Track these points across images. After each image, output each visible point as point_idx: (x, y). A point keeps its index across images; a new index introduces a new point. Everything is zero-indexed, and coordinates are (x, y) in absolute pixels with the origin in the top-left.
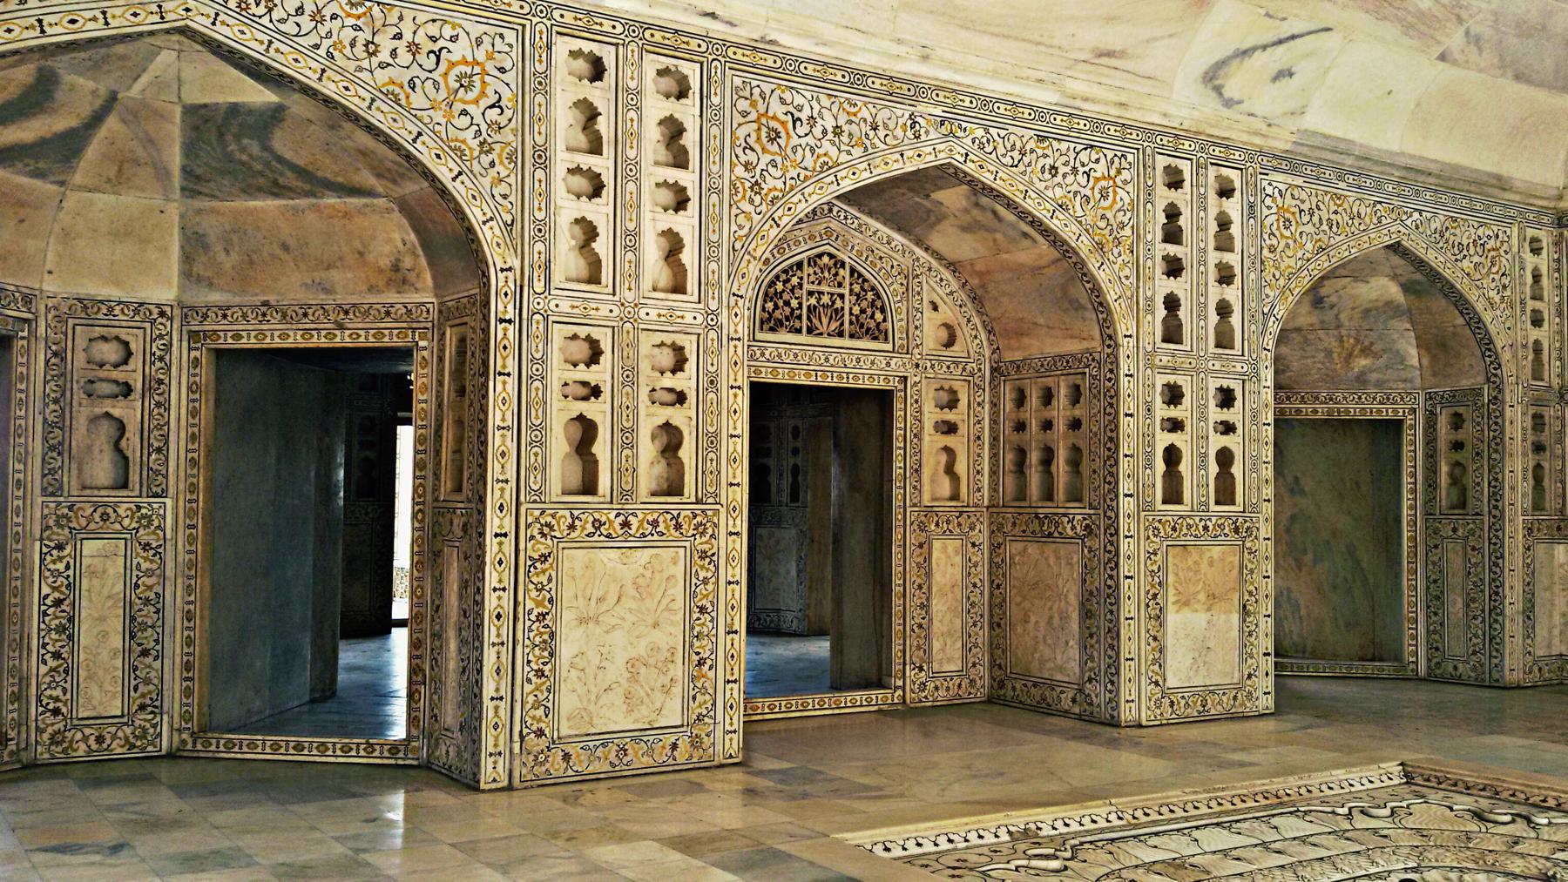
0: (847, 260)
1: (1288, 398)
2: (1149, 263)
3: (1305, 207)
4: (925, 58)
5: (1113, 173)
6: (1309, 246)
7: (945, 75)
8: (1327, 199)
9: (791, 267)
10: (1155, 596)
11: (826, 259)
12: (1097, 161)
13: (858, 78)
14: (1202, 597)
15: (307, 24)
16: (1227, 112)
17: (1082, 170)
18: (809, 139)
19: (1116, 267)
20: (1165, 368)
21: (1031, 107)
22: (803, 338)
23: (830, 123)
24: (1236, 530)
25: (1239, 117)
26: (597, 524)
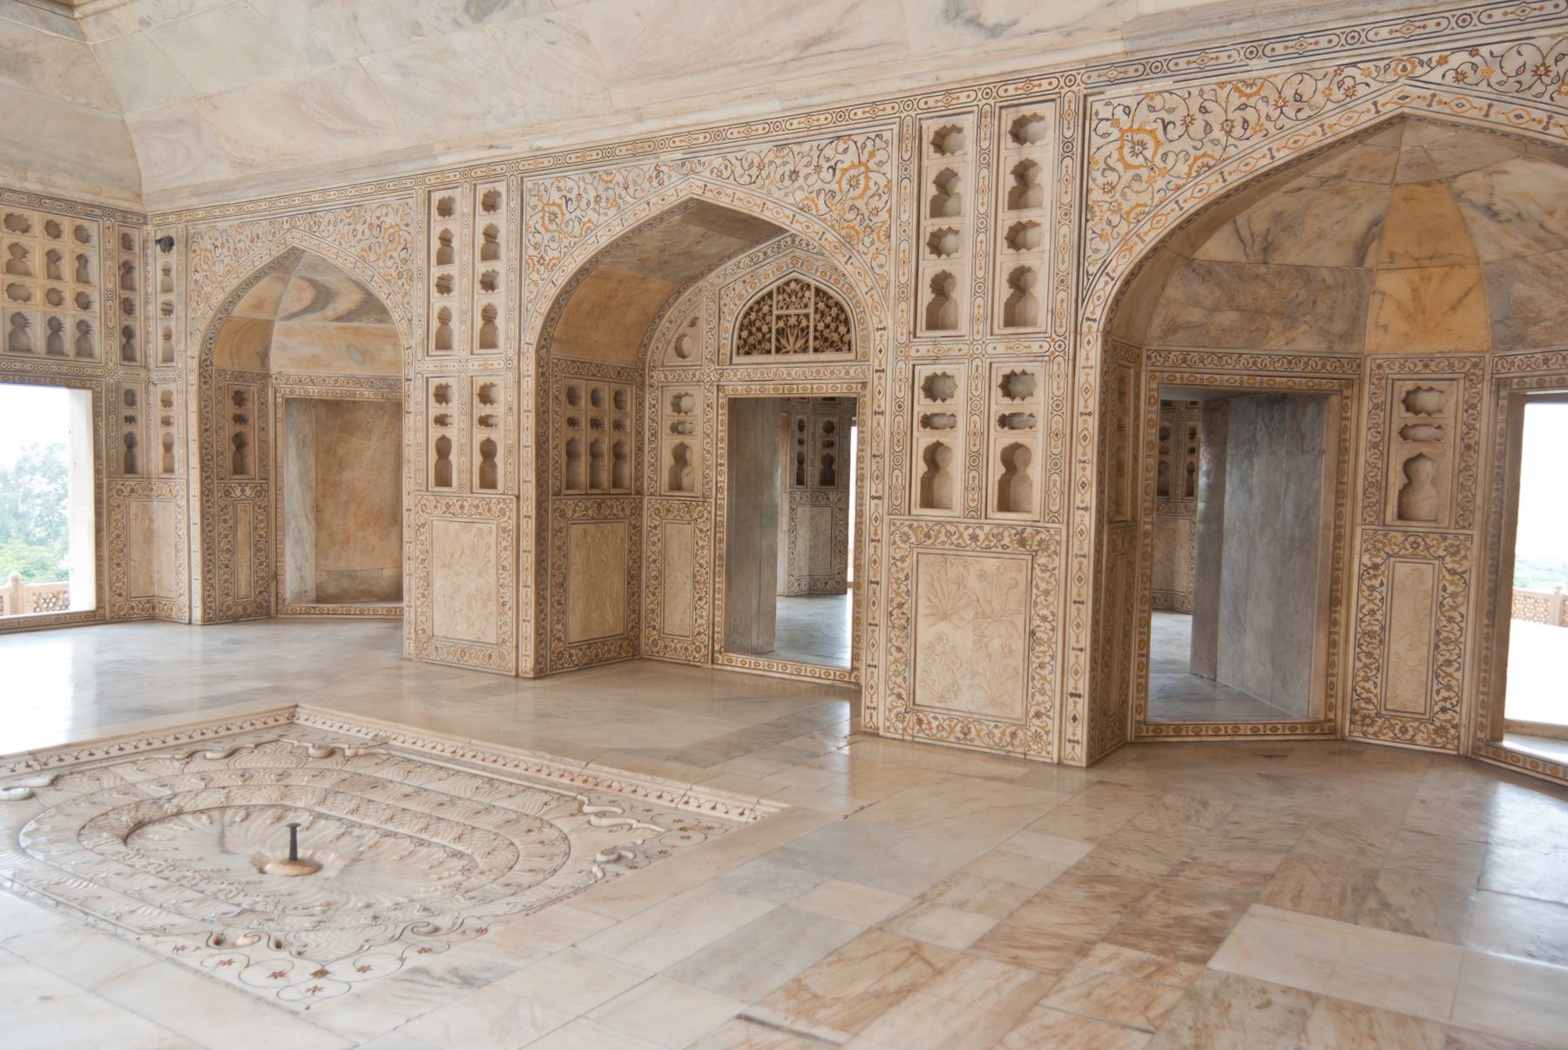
0: (813, 283)
1: (1546, 361)
2: (905, 245)
3: (1177, 117)
4: (639, 119)
5: (864, 158)
6: (1182, 168)
7: (669, 123)
8: (1222, 94)
9: (763, 298)
10: (901, 605)
11: (793, 285)
12: (845, 151)
13: (607, 152)
14: (969, 615)
15: (331, 228)
16: (995, 44)
17: (826, 165)
18: (578, 213)
19: (868, 258)
20: (923, 358)
21: (765, 121)
22: (774, 357)
23: (592, 195)
24: (1022, 542)
25: (1014, 42)
26: (448, 506)
